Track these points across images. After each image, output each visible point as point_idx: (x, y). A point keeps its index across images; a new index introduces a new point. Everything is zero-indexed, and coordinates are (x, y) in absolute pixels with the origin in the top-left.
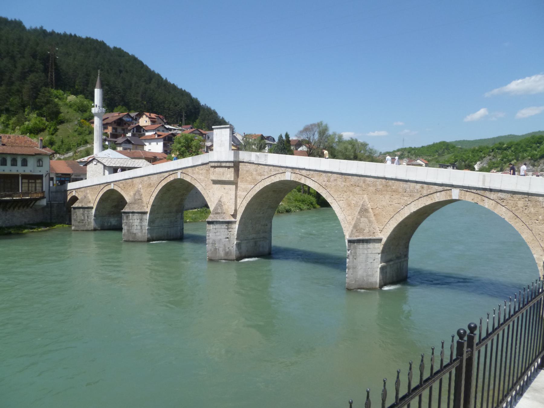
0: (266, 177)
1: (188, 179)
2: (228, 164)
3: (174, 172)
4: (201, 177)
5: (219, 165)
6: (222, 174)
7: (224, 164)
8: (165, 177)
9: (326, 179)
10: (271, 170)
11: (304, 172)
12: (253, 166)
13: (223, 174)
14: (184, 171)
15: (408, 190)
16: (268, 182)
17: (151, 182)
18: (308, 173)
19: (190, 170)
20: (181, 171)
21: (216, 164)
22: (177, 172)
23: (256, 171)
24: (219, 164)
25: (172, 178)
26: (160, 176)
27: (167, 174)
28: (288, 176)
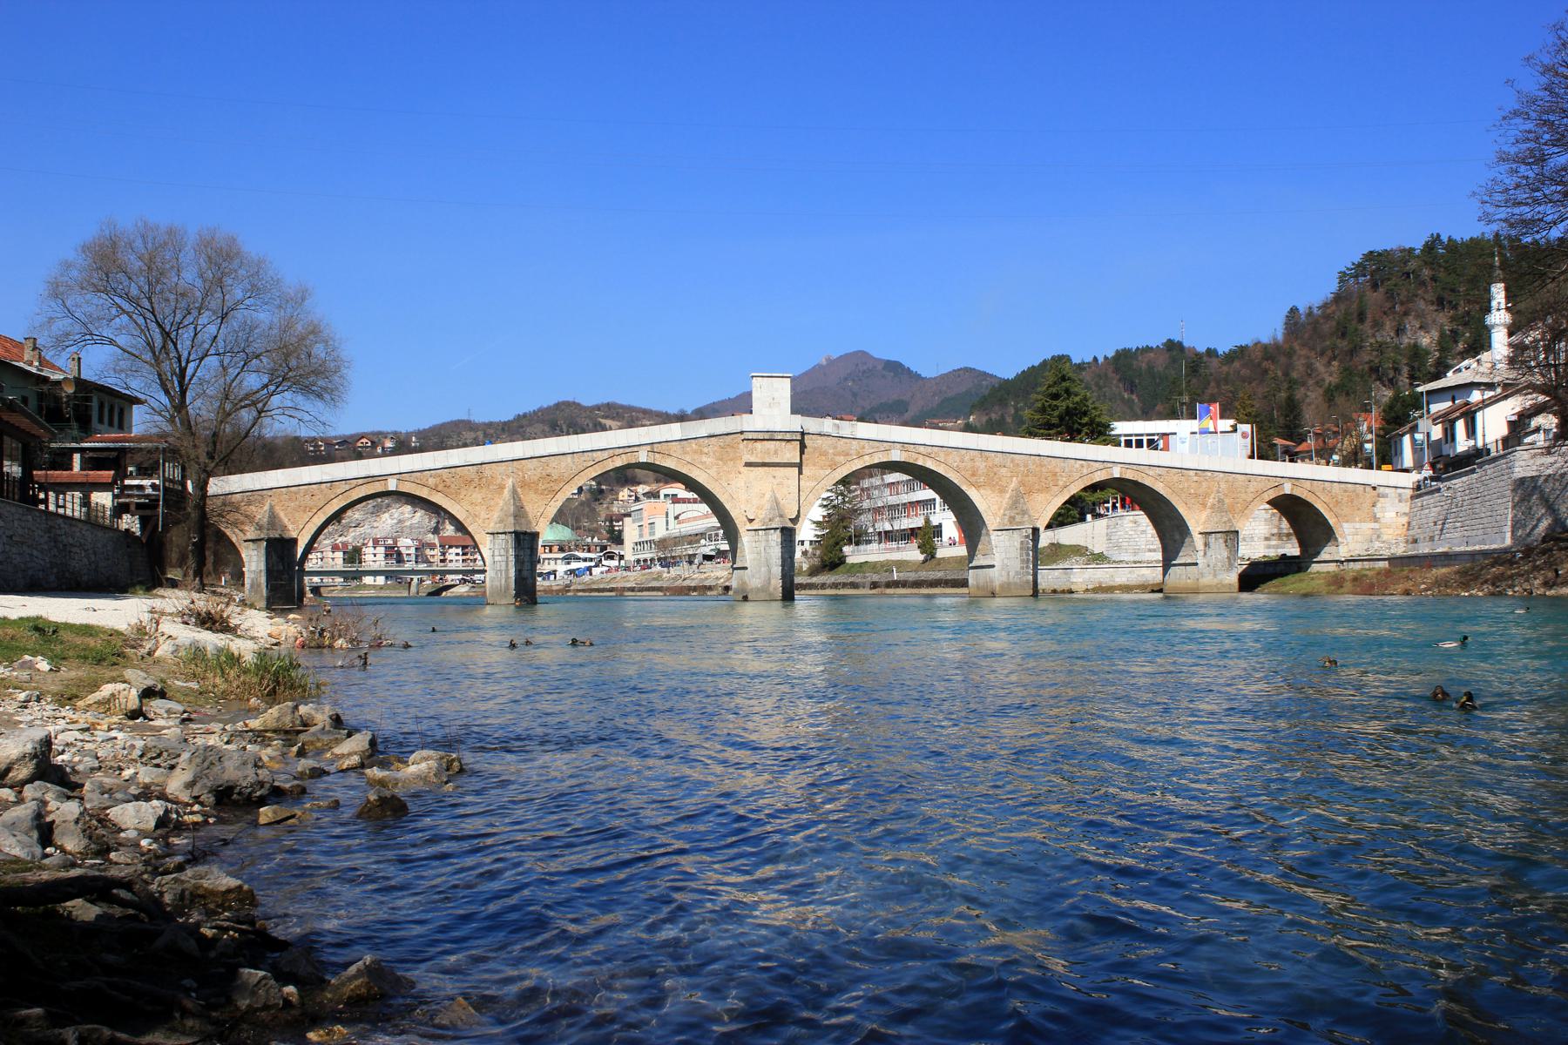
2: (788, 437)
3: (630, 450)
5: (770, 437)
9: (958, 459)
10: (864, 448)
11: (922, 449)
12: (830, 441)
13: (776, 452)
15: (1067, 470)
18: (929, 449)
20: (649, 448)
21: (760, 436)
22: (635, 449)
24: (767, 436)
25: (619, 462)
26: (583, 459)
27: (606, 455)
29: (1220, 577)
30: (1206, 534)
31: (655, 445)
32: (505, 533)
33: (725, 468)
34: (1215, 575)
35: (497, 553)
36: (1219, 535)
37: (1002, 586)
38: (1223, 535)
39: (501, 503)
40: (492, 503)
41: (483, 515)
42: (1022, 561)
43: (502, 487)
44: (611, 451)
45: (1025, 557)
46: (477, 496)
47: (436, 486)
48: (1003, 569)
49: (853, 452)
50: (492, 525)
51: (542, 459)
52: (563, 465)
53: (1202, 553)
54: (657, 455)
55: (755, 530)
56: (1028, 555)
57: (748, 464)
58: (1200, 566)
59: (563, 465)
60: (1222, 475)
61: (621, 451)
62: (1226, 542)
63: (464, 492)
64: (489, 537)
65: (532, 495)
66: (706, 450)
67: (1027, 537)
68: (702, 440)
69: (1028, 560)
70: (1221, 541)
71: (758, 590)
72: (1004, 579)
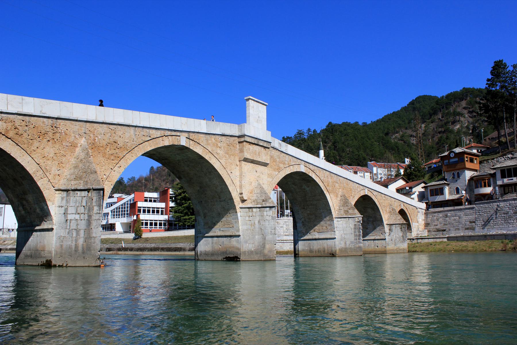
0: (287, 166)
1: (198, 150)
3: (174, 133)
4: (219, 151)
6: (257, 154)
7: (261, 143)
8: (152, 137)
11: (311, 166)
14: (192, 136)
16: (288, 171)
17: (116, 138)
19: (202, 137)
20: (186, 135)
22: (178, 134)
23: (279, 158)
24: (256, 141)
25: (167, 142)
26: (143, 133)
27: (158, 133)
28: (303, 169)
29: (398, 245)
30: (391, 225)
31: (191, 134)
32: (88, 190)
33: (230, 160)
34: (395, 245)
35: (71, 210)
36: (398, 225)
37: (341, 250)
38: (400, 225)
39: (73, 161)
40: (64, 159)
41: (54, 170)
42: (355, 236)
43: (74, 146)
44: (163, 132)
45: (357, 233)
46: (50, 150)
47: (7, 131)
48: (341, 240)
49: (286, 162)
50: (62, 182)
51: (112, 127)
52: (127, 135)
53: (388, 234)
54: (191, 142)
55: (249, 208)
56: (360, 232)
57: (246, 160)
58: (387, 240)
59: (127, 135)
60: (389, 198)
61: (169, 133)
62: (401, 228)
63: (36, 144)
64: (58, 196)
65: (100, 158)
66: (219, 145)
67: (359, 222)
68: (217, 137)
69: (360, 235)
70: (399, 228)
71: (251, 252)
72: (343, 245)
